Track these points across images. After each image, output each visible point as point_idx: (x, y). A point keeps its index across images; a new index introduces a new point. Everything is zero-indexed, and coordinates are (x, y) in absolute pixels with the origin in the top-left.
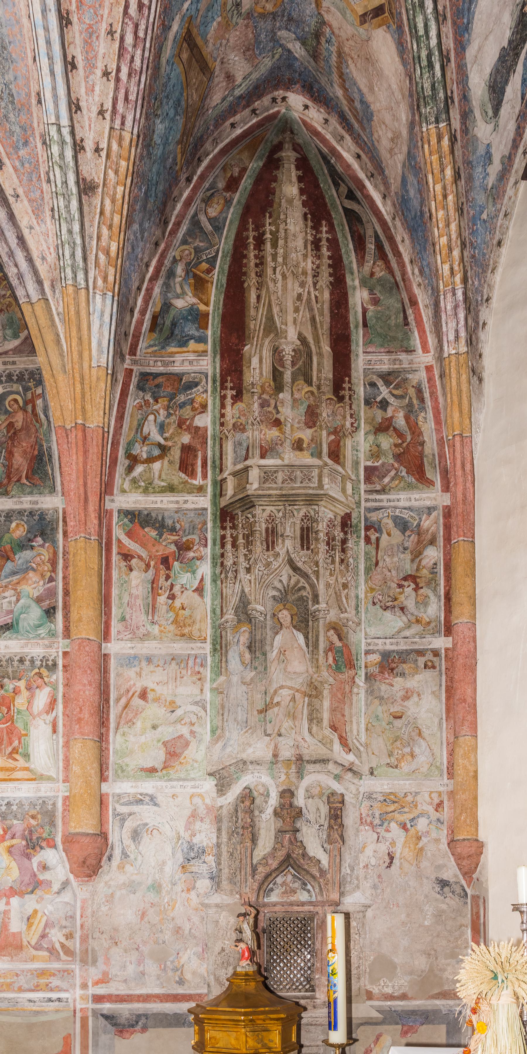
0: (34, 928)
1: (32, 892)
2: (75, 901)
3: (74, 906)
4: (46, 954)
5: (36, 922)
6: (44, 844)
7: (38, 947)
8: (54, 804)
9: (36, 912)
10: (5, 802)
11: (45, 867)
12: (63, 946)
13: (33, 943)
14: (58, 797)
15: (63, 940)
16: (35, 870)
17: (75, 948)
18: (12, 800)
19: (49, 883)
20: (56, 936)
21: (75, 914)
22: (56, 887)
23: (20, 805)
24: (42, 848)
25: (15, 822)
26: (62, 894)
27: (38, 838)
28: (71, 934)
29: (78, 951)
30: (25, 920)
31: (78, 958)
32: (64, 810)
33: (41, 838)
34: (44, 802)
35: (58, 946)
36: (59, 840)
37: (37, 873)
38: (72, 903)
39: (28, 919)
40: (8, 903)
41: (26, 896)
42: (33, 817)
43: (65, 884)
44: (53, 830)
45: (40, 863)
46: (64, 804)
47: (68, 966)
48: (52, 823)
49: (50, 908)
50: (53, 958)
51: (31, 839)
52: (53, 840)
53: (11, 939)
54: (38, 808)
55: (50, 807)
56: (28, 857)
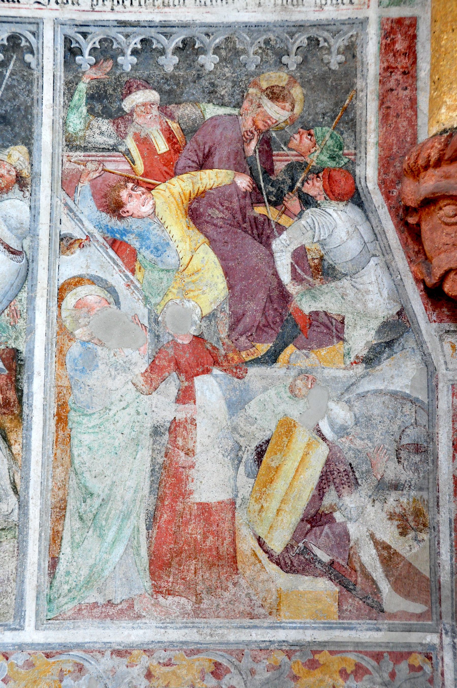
0: (280, 486)
1: (272, 358)
2: (432, 389)
3: (430, 411)
4: (324, 586)
5: (289, 466)
6: (314, 188)
7: (295, 561)
8: (351, 51)
9: (287, 427)
10: (177, 41)
11: (317, 268)
12: (388, 556)
13: (277, 545)
14: (364, 22)
15: (388, 534)
16: (286, 277)
17: (435, 567)
18: (198, 32)
19: (330, 329)
20: (365, 520)
21: (431, 438)
22: (360, 338)
23: (230, 52)
24: (307, 201)
25: (211, 111)
26: (385, 366)
27: (293, 169)
28: (418, 513)
29: (445, 576)
30: (249, 456)
31: (446, 607)
32: (389, 69)
33: (302, 166)
34: (314, 42)
35: (368, 556)
36: (369, 173)
37: (292, 288)
38: (422, 397)
39: (260, 453)
40: (186, 396)
41: (254, 371)
42: (275, 95)
43: (395, 332)
44: (347, 138)
45: (300, 255)
46: (387, 48)
47: (414, 638)
48: (346, 120)
49: (341, 413)
50: (351, 603)
51: (269, 171)
52: (351, 174)
53: (194, 530)
54: (292, 61)
55: (335, 60)
56: (263, 233)
